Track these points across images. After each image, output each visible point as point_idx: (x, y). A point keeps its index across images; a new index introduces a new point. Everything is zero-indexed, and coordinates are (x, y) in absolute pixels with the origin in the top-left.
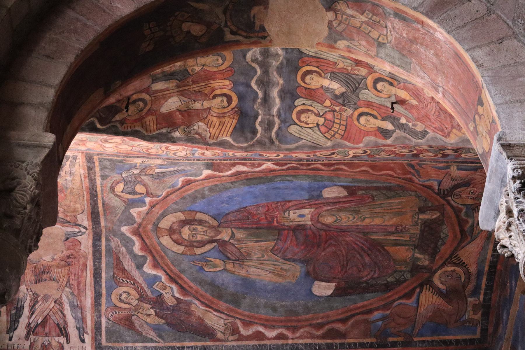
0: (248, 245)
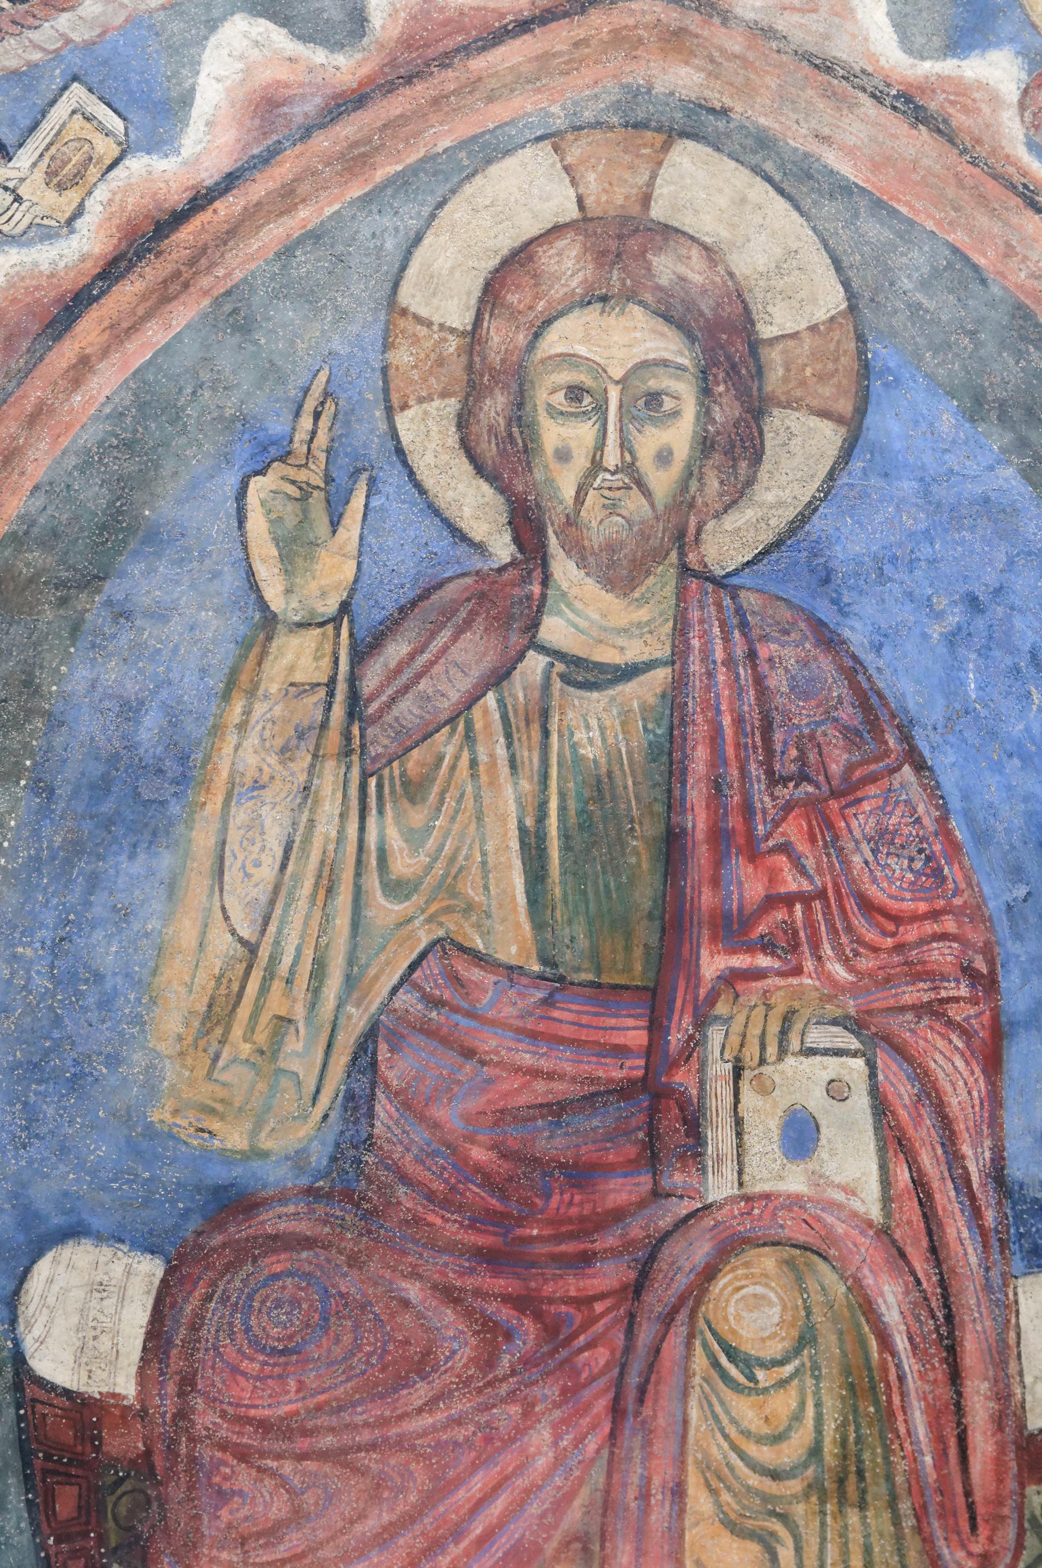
0: (493, 783)
